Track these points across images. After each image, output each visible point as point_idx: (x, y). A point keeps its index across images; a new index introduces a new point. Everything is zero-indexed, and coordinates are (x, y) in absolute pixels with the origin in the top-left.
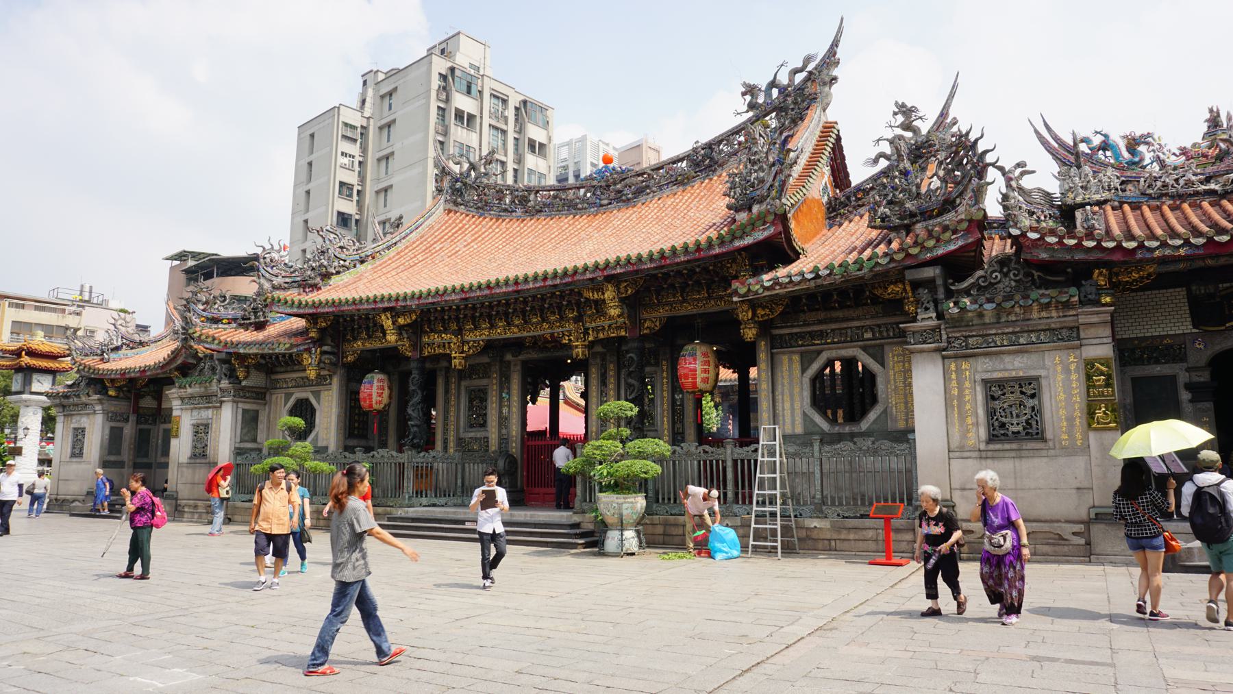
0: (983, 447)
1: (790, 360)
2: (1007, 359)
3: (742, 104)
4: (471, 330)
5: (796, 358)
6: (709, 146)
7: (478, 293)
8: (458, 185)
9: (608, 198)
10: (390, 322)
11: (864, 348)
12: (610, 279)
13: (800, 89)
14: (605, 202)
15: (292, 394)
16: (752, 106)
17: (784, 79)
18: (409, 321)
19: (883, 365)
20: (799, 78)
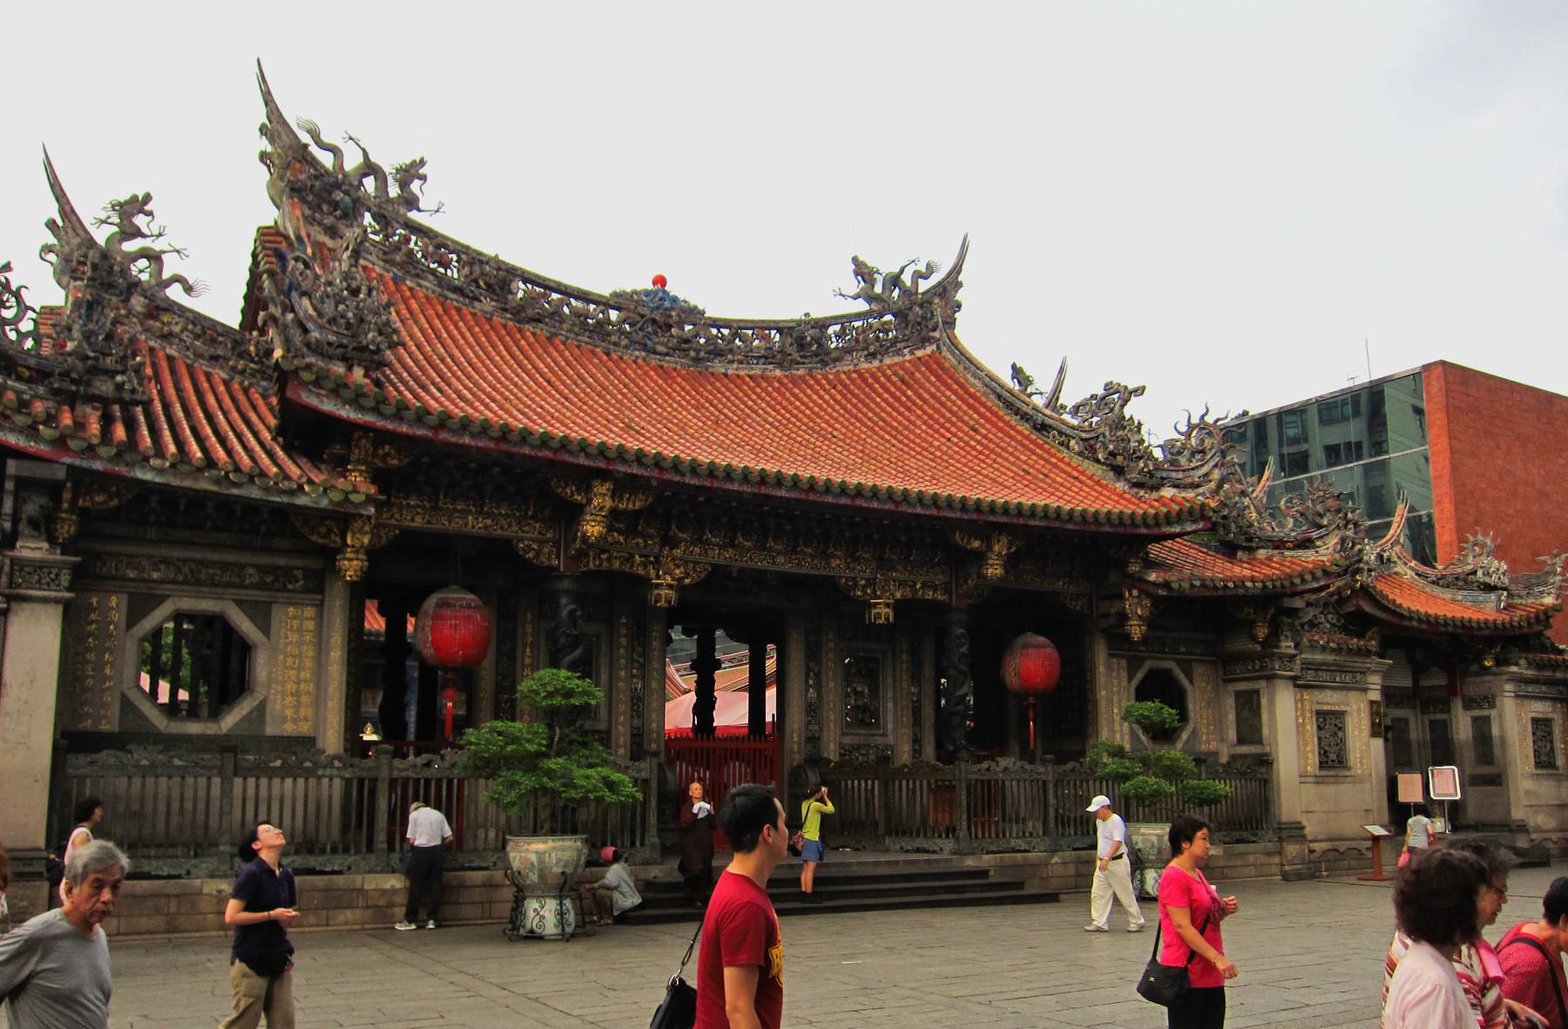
2: (1329, 693)
3: (853, 286)
4: (698, 540)
5: (1124, 663)
6: (822, 325)
7: (783, 493)
9: (662, 344)
10: (608, 503)
11: (1179, 662)
12: (1001, 528)
13: (926, 303)
14: (663, 349)
15: (159, 600)
17: (907, 279)
18: (638, 505)
19: (1191, 682)
20: (924, 285)
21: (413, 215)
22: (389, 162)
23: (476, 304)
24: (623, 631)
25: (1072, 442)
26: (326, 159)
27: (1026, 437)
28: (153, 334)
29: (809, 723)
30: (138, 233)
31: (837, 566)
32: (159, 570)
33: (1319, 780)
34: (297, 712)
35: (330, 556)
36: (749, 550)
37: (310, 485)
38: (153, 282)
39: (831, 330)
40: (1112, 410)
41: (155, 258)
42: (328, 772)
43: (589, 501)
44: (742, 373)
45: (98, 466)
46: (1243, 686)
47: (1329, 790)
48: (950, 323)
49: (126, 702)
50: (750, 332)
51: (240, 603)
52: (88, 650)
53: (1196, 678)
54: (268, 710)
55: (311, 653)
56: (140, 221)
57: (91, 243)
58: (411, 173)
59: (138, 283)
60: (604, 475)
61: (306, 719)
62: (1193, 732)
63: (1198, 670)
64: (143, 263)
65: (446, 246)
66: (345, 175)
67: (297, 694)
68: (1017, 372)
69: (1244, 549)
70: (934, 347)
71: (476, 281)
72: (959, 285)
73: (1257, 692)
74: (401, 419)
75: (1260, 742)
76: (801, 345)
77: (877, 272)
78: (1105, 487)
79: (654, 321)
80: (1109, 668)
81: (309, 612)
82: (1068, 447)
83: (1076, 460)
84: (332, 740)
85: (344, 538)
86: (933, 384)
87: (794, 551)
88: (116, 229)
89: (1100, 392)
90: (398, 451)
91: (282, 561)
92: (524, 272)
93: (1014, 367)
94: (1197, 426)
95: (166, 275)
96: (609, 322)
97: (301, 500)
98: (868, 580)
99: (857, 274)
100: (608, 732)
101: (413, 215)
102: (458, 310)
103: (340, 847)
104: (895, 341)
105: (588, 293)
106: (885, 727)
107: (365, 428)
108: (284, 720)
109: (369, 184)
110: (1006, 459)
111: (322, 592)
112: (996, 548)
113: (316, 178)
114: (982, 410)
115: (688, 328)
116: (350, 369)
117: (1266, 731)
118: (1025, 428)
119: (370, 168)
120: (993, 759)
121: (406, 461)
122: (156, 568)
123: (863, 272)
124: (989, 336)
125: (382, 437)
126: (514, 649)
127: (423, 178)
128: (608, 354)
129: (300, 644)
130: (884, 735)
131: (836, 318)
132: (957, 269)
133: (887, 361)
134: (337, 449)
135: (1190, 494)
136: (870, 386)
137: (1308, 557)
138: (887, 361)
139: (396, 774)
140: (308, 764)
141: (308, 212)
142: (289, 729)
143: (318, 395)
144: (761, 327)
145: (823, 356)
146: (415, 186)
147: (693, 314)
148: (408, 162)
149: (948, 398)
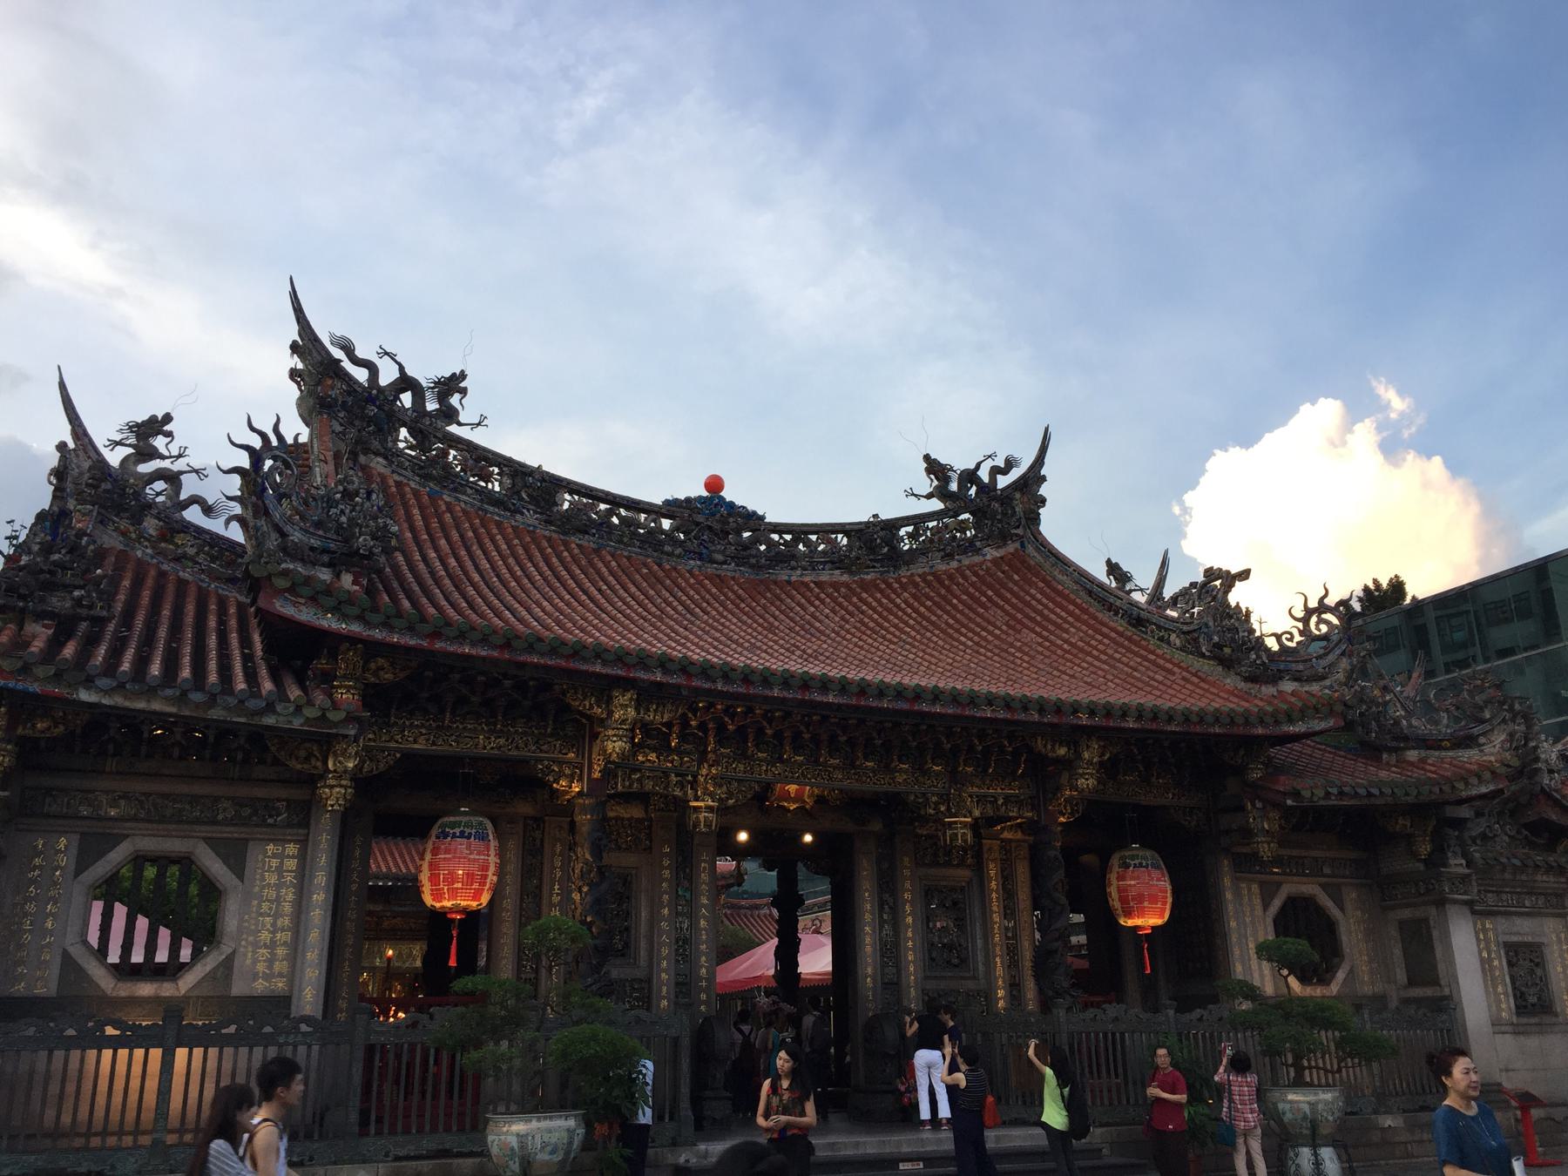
0: (1515, 1020)
1: (1249, 890)
2: (1518, 921)
3: (925, 484)
5: (1255, 887)
6: (893, 525)
8: (372, 410)
9: (719, 552)
10: (631, 712)
11: (1323, 886)
12: (1089, 732)
14: (720, 557)
15: (115, 840)
16: (941, 492)
19: (1342, 909)
20: (1003, 482)
21: (453, 429)
22: (425, 373)
23: (518, 517)
24: (666, 863)
25: (1173, 636)
26: (361, 375)
27: (1121, 634)
28: (165, 557)
29: (884, 965)
30: (154, 454)
31: (902, 778)
32: (117, 806)
33: (1518, 1031)
34: (270, 967)
35: (312, 781)
36: (801, 765)
37: (293, 708)
38: (169, 504)
39: (902, 532)
40: (1214, 598)
41: (173, 478)
42: (291, 1039)
43: (610, 713)
44: (807, 579)
45: (35, 687)
46: (1406, 914)
47: (1532, 1042)
48: (1035, 519)
49: (68, 962)
50: (814, 537)
51: (207, 840)
52: (29, 899)
53: (1349, 906)
54: (236, 963)
55: (290, 897)
56: (159, 442)
57: (101, 462)
58: (452, 385)
59: (150, 505)
60: (626, 684)
61: (281, 975)
62: (1351, 971)
63: (1351, 896)
64: (160, 485)
65: (486, 459)
66: (381, 390)
67: (272, 946)
68: (1113, 568)
69: (1391, 750)
70: (1017, 545)
71: (518, 493)
72: (1044, 479)
73: (1426, 920)
74: (391, 629)
75: (1435, 982)
76: (871, 548)
77: (951, 469)
78: (1213, 684)
79: (710, 528)
80: (1238, 894)
81: (292, 849)
82: (1169, 643)
83: (1179, 656)
84: (309, 999)
85: (325, 763)
86: (1016, 583)
87: (853, 766)
88: (131, 450)
89: (1200, 578)
90: (392, 664)
91: (260, 792)
92: (569, 482)
93: (1109, 562)
94: (1314, 611)
95: (183, 496)
96: (663, 532)
97: (270, 720)
98: (940, 796)
99: (929, 471)
100: (649, 981)
101: (453, 429)
102: (499, 525)
103: (302, 1134)
104: (971, 541)
105: (638, 502)
106: (976, 969)
107: (353, 640)
108: (255, 977)
109: (406, 399)
110: (1097, 658)
111: (307, 826)
112: (1086, 755)
113: (349, 393)
114: (1071, 607)
115: (746, 535)
116: (338, 576)
117: (1441, 967)
118: (1120, 624)
119: (406, 382)
120: (1098, 1006)
121: (402, 675)
122: (114, 804)
123: (935, 468)
124: (1075, 528)
125: (372, 649)
126: (540, 887)
127: (464, 392)
128: (660, 565)
129: (278, 887)
130: (975, 978)
131: (907, 518)
132: (1040, 461)
133: (966, 562)
134: (322, 664)
135: (1315, 688)
136: (948, 589)
137: (1468, 756)
138: (966, 562)
139: (373, 1039)
140: (268, 1029)
141: (339, 429)
142: (260, 987)
143: (295, 604)
144: (826, 530)
145: (896, 558)
146: (455, 400)
147: (752, 519)
148: (447, 375)
149: (1033, 597)
